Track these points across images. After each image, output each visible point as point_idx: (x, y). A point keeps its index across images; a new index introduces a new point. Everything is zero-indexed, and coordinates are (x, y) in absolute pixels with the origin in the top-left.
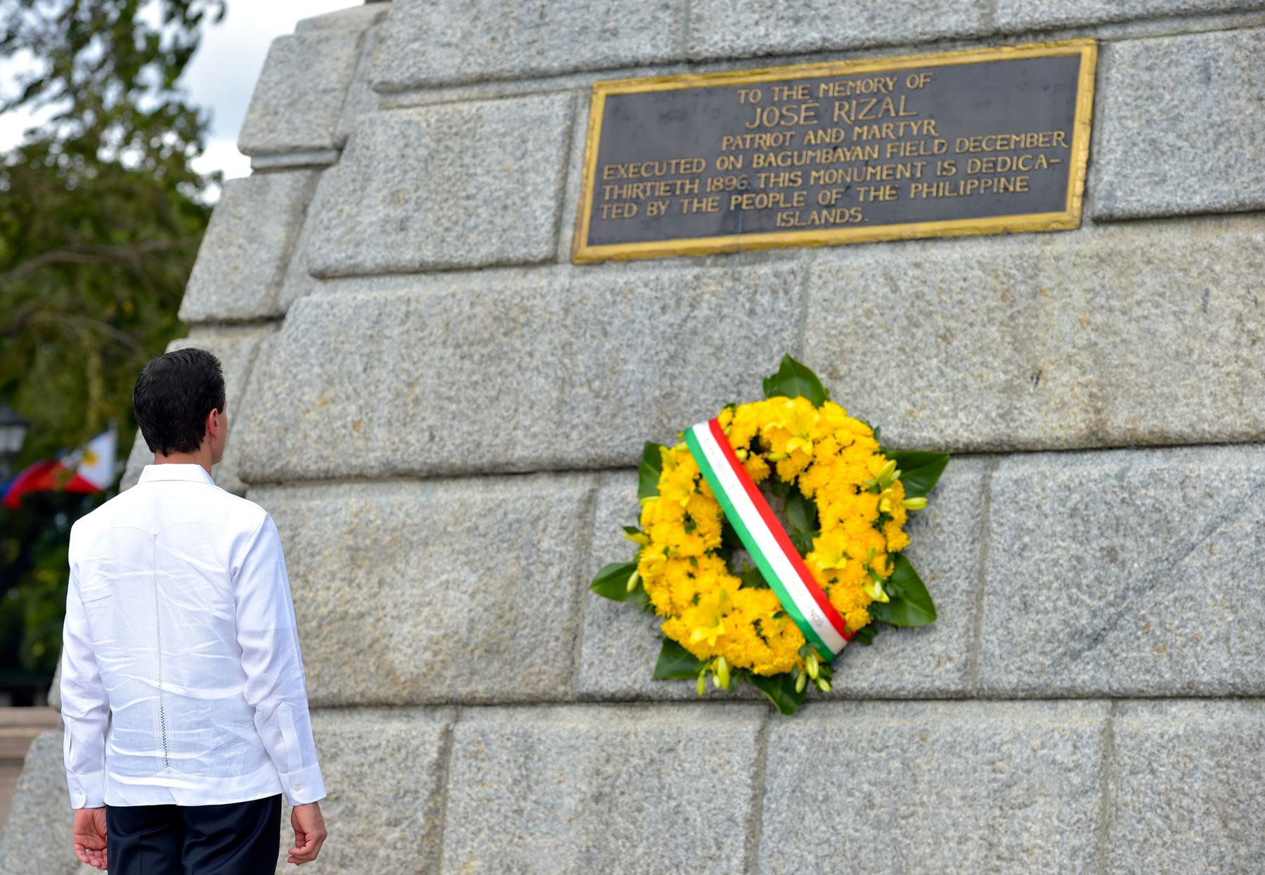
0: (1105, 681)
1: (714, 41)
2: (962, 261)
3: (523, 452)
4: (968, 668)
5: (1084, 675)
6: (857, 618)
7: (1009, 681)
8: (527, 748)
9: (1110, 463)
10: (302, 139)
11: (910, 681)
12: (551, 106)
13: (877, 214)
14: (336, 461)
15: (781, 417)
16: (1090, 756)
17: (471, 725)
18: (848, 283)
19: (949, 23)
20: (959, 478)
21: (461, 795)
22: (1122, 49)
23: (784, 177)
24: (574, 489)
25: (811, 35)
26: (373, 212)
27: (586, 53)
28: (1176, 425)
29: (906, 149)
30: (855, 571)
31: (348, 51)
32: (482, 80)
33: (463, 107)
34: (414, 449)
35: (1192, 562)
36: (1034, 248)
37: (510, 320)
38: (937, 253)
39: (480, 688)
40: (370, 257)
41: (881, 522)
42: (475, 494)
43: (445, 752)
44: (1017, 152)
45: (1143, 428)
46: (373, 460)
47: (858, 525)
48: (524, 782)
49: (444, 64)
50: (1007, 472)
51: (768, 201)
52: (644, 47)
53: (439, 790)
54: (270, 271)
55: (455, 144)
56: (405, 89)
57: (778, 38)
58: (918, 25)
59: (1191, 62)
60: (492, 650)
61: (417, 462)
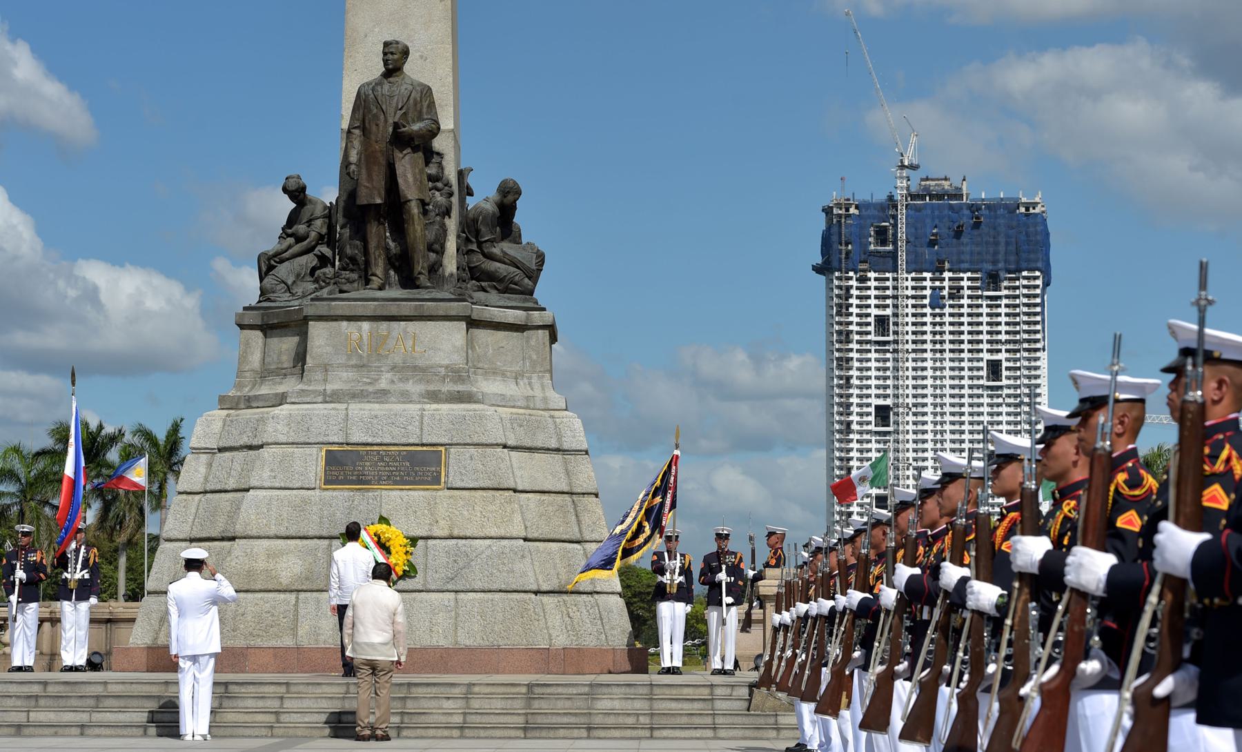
0: (454, 588)
1: (354, 439)
2: (417, 495)
3: (311, 534)
4: (424, 585)
5: (450, 587)
6: (401, 573)
7: (433, 588)
8: (318, 601)
9: (454, 541)
11: (411, 587)
12: (314, 450)
13: (396, 483)
14: (262, 534)
15: (382, 528)
16: (452, 604)
17: (302, 595)
18: (392, 498)
19: (411, 441)
20: (420, 543)
21: (302, 612)
24: (326, 542)
25: (378, 441)
26: (266, 474)
27: (321, 440)
28: (468, 535)
30: (400, 563)
31: (220, 424)
33: (290, 449)
34: (283, 532)
35: (473, 563)
36: (434, 493)
37: (305, 501)
38: (415, 493)
39: (304, 588)
40: (266, 484)
41: (407, 552)
42: (298, 542)
43: (297, 602)
45: (461, 534)
46: (271, 533)
47: (402, 554)
48: (318, 608)
49: (283, 439)
50: (430, 542)
52: (336, 440)
53: (296, 610)
57: (370, 440)
58: (404, 441)
60: (307, 579)
61: (283, 534)
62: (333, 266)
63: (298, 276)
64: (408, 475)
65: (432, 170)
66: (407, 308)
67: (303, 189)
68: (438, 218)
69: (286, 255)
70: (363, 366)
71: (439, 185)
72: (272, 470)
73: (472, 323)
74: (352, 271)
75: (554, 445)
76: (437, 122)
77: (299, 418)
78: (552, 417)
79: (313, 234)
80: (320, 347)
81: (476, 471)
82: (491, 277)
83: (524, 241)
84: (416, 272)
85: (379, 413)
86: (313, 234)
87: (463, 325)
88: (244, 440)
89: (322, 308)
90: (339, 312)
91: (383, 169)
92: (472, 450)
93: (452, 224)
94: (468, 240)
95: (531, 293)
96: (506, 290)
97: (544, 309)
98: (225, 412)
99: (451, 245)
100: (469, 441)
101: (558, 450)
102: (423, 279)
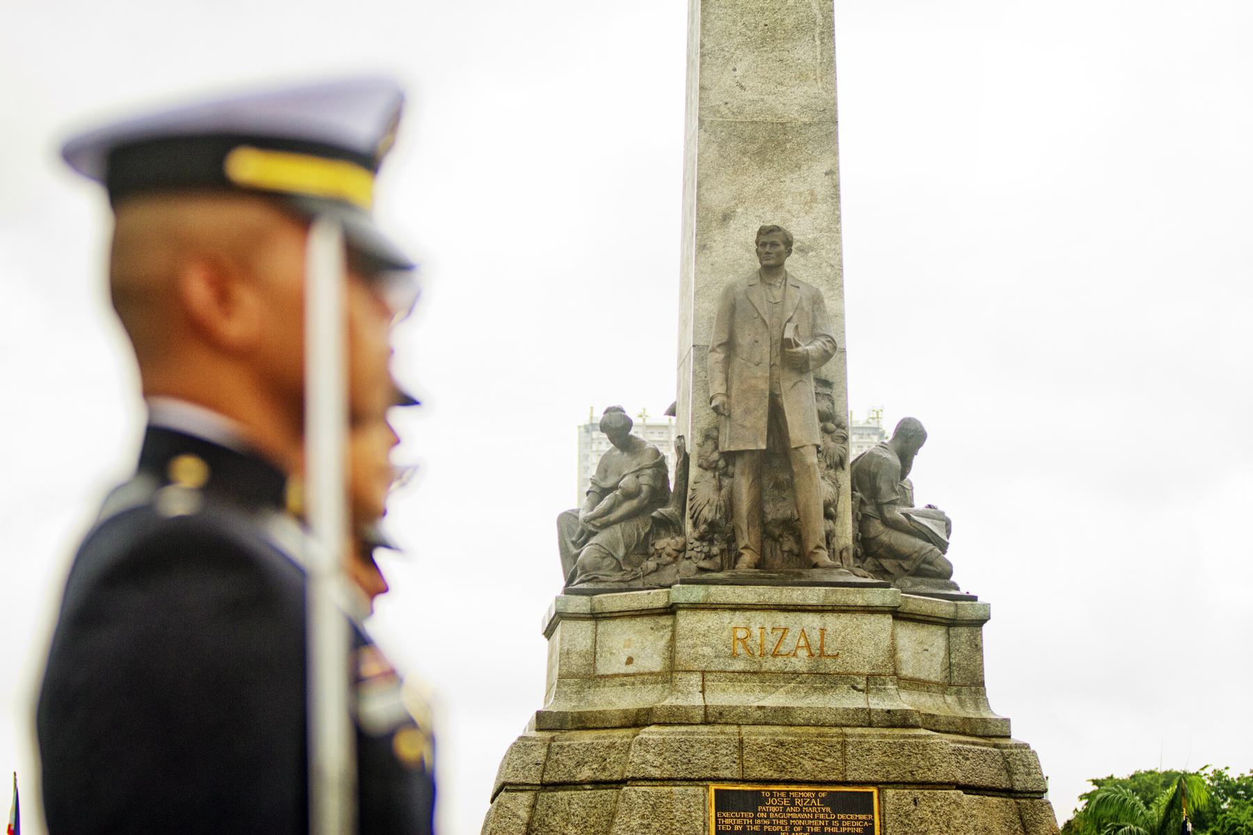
1: (754, 774)
10: (530, 781)
19: (832, 777)
22: (890, 792)
23: (781, 822)
25: (787, 777)
29: (822, 816)
31: (545, 750)
32: (669, 779)
44: (858, 820)
49: (656, 773)
51: (777, 829)
54: (523, 828)
55: (664, 801)
56: (640, 779)
57: (776, 776)
58: (822, 776)
59: (910, 799)
62: (680, 532)
63: (627, 547)
64: (830, 825)
65: (825, 405)
66: (813, 595)
67: (629, 424)
68: (832, 472)
69: (613, 517)
70: (755, 673)
71: (831, 426)
72: (643, 817)
73: (899, 615)
74: (711, 542)
75: (1002, 782)
76: (832, 341)
77: (676, 745)
78: (995, 746)
79: (645, 488)
80: (694, 646)
81: (922, 821)
82: (893, 553)
83: (919, 503)
84: (811, 547)
85: (784, 738)
86: (645, 488)
87: (888, 620)
88: (585, 774)
89: (697, 593)
90: (721, 599)
91: (767, 400)
92: (917, 793)
93: (845, 478)
94: (862, 502)
95: (950, 574)
96: (918, 573)
97: (974, 598)
98: (547, 735)
99: (846, 508)
100: (909, 778)
101: (1009, 792)
102: (824, 557)
